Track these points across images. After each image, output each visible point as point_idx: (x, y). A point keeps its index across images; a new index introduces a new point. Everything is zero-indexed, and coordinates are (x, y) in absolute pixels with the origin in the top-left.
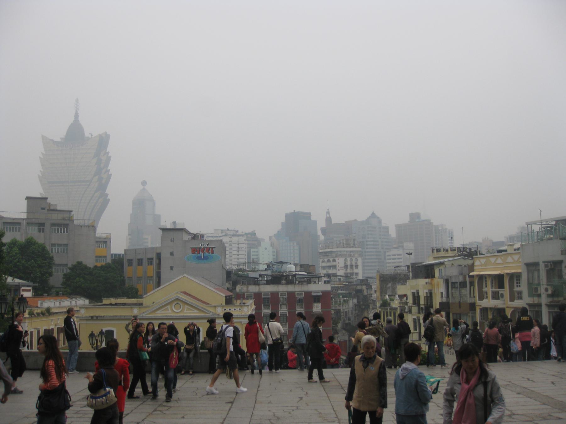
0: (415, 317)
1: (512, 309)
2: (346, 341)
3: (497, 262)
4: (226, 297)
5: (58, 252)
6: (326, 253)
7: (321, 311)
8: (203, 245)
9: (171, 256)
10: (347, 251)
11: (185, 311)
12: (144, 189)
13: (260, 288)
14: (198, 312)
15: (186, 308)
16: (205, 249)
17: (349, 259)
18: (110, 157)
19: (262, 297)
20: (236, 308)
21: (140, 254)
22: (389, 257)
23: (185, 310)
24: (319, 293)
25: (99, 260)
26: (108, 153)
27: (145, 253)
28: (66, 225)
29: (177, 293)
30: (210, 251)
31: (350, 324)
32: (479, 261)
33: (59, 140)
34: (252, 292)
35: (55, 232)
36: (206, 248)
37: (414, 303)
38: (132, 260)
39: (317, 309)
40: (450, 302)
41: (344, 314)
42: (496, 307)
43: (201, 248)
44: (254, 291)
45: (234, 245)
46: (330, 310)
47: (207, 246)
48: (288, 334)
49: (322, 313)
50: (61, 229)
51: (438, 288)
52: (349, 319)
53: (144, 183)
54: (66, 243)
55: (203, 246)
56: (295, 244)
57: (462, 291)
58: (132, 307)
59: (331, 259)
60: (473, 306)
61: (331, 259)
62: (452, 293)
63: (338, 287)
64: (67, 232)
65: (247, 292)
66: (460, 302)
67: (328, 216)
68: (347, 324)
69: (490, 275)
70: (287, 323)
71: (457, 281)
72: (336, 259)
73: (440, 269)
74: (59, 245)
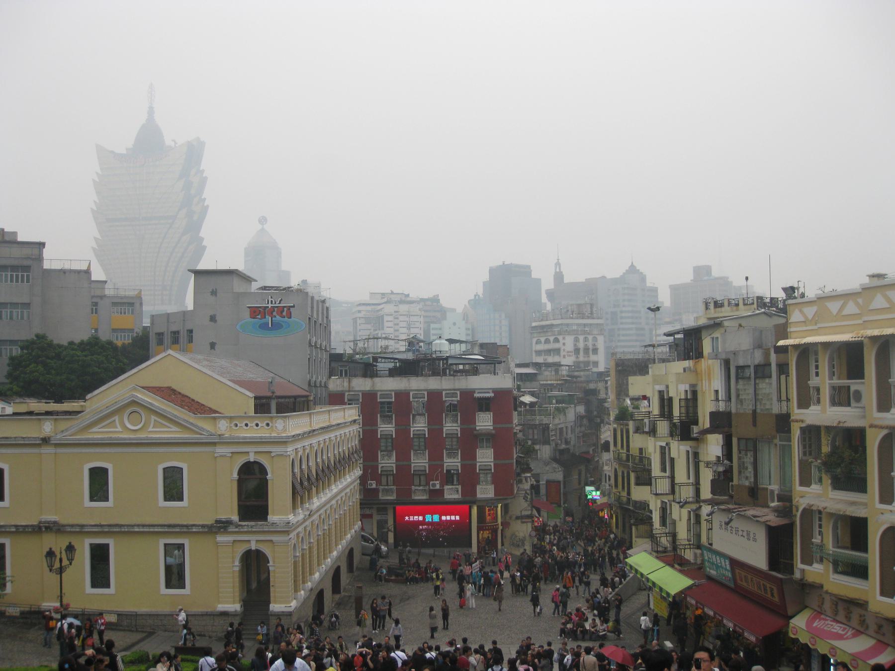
0: (664, 444)
1: (885, 432)
2: (559, 482)
3: (846, 312)
4: (256, 398)
5: (11, 318)
6: (543, 327)
7: (491, 428)
8: (272, 301)
9: (212, 323)
10: (578, 325)
11: (151, 429)
12: (263, 229)
13: (373, 382)
14: (178, 429)
15: (153, 421)
16: (276, 309)
17: (581, 338)
18: (206, 178)
19: (379, 400)
20: (259, 423)
21: (175, 322)
23: (149, 426)
24: (488, 392)
25: (121, 336)
26: (203, 171)
27: (184, 320)
28: (27, 268)
29: (134, 389)
30: (284, 313)
31: (568, 449)
32: (801, 311)
33: (125, 152)
34: (358, 391)
35: (6, 281)
36: (277, 307)
37: (662, 415)
38: (162, 334)
39: (419, 425)
40: (733, 411)
41: (556, 432)
42: (841, 425)
43: (268, 307)
44: (363, 388)
45: (401, 318)
46: (510, 426)
47: (280, 303)
48: (427, 472)
49: (493, 432)
50: (17, 276)
51: (710, 380)
52: (567, 443)
53: (263, 220)
54: (26, 301)
55: (272, 303)
56: (503, 316)
57: (761, 386)
58: (40, 420)
59: (552, 339)
60: (783, 422)
61: (552, 339)
62: (737, 390)
63: (552, 385)
64: (28, 281)
65: (349, 391)
66: (754, 412)
67: (558, 270)
68: (562, 452)
69: (826, 345)
70: (427, 451)
71: (749, 363)
72: (560, 338)
73: (713, 338)
74: (14, 305)
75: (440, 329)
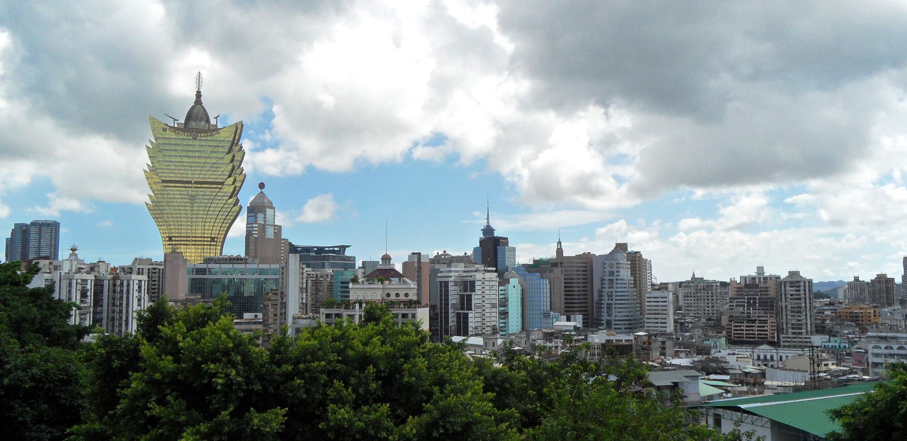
12: (262, 192)
22: (649, 300)
45: (487, 283)
53: (262, 186)
56: (548, 281)
67: (559, 247)
75: (505, 290)
